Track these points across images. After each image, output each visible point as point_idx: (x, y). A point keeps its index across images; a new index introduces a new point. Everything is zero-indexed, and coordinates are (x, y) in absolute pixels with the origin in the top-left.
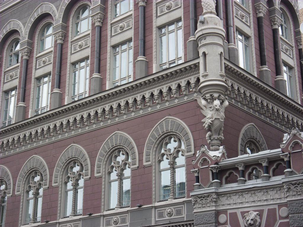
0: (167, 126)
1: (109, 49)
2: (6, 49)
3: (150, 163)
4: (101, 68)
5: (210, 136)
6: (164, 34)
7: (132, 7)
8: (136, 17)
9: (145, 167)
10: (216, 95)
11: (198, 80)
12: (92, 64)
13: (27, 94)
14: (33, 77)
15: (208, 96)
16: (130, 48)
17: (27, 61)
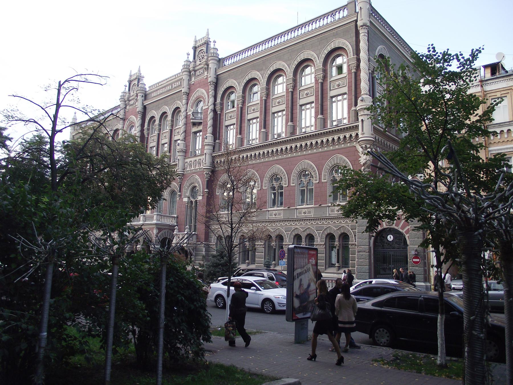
0: (337, 159)
1: (298, 107)
2: (225, 98)
3: (326, 181)
4: (294, 119)
5: (364, 169)
6: (335, 102)
7: (313, 80)
8: (317, 88)
9: (323, 183)
10: (368, 146)
11: (357, 134)
12: (287, 115)
13: (242, 130)
14: (246, 119)
15: (364, 146)
16: (312, 108)
17: (242, 108)
